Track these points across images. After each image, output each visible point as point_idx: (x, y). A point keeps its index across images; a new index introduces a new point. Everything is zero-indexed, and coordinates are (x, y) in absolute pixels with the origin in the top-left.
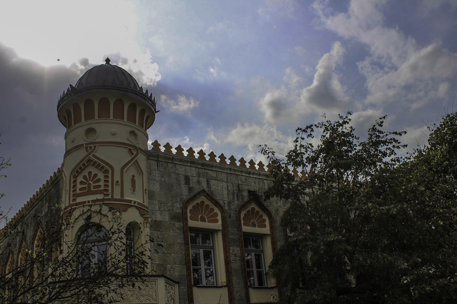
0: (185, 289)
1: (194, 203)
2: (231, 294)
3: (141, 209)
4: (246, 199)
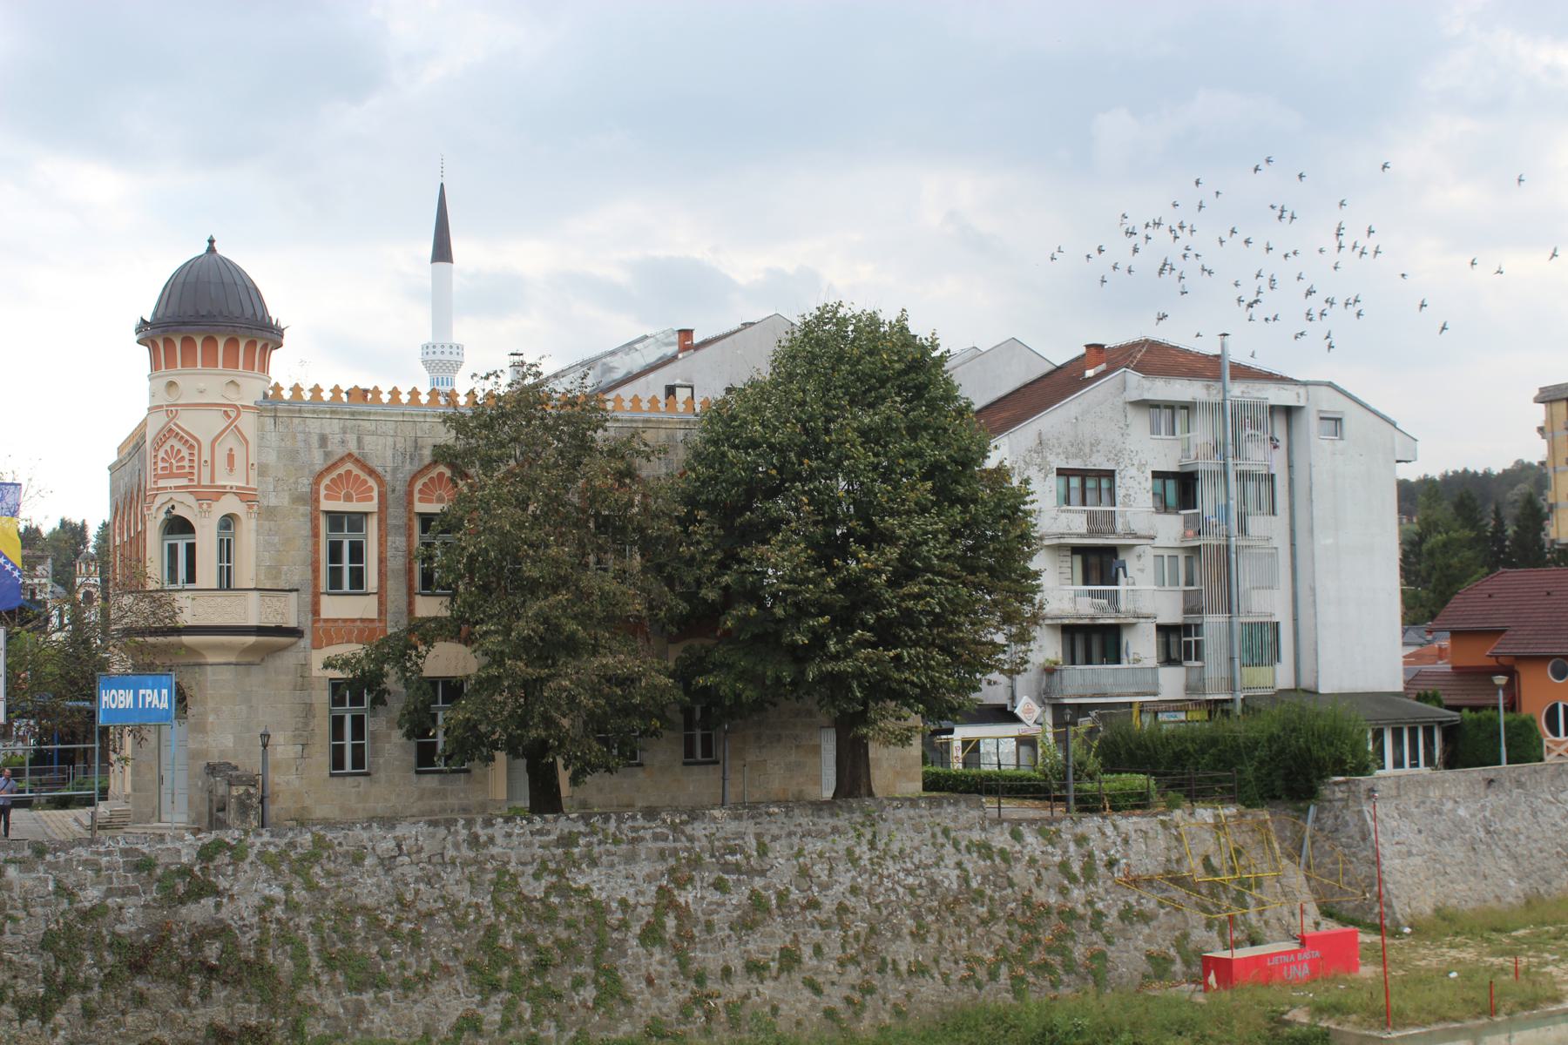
0: (307, 597)
1: (334, 475)
2: (381, 604)
3: (244, 496)
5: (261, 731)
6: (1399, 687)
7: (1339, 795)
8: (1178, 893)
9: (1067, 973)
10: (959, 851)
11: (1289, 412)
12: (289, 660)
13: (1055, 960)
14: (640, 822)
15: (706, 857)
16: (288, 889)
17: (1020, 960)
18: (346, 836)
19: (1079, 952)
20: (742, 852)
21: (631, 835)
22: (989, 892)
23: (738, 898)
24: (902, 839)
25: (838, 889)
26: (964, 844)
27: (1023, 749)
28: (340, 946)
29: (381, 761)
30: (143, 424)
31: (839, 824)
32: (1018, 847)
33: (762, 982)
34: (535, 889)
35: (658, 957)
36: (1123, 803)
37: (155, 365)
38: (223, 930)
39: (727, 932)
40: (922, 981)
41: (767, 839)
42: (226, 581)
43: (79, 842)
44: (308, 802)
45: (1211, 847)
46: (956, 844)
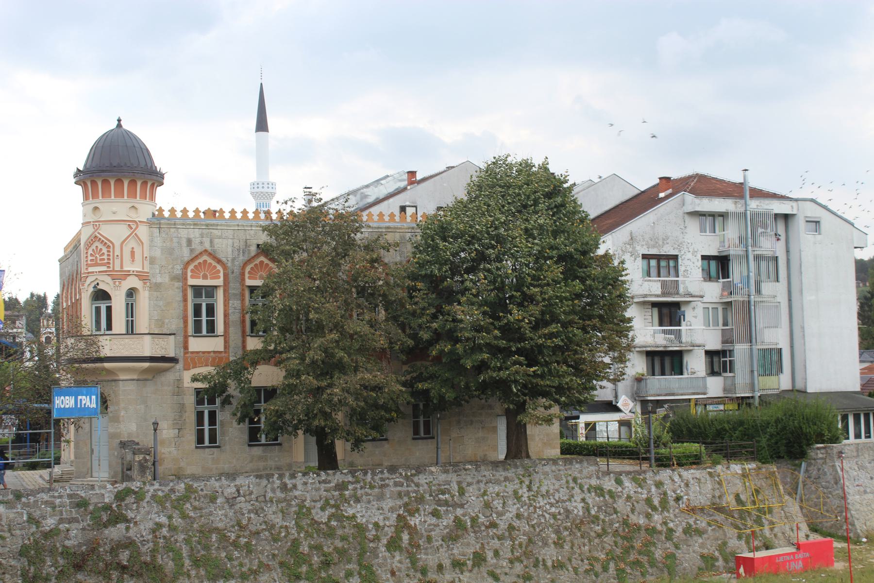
0: (181, 339)
1: (196, 263)
3: (142, 276)
4: (253, 254)
5: (153, 421)
6: (858, 388)
7: (820, 456)
8: (720, 517)
9: (651, 567)
10: (583, 491)
11: (786, 217)
12: (170, 377)
13: (644, 559)
14: (386, 475)
15: (427, 496)
16: (170, 518)
17: (622, 560)
18: (205, 485)
19: (658, 554)
20: (449, 493)
21: (380, 483)
22: (602, 517)
23: (447, 521)
24: (548, 485)
25: (508, 515)
26: (586, 487)
27: (623, 429)
28: (203, 553)
29: (227, 438)
30: (79, 234)
31: (509, 475)
32: (620, 489)
33: (462, 573)
34: (322, 517)
35: (398, 558)
36: (684, 461)
37: (86, 197)
38: (131, 543)
39: (440, 542)
40: (561, 572)
41: (464, 485)
42: (131, 330)
43: (42, 490)
44: (182, 464)
45: (739, 488)
46: (581, 488)
